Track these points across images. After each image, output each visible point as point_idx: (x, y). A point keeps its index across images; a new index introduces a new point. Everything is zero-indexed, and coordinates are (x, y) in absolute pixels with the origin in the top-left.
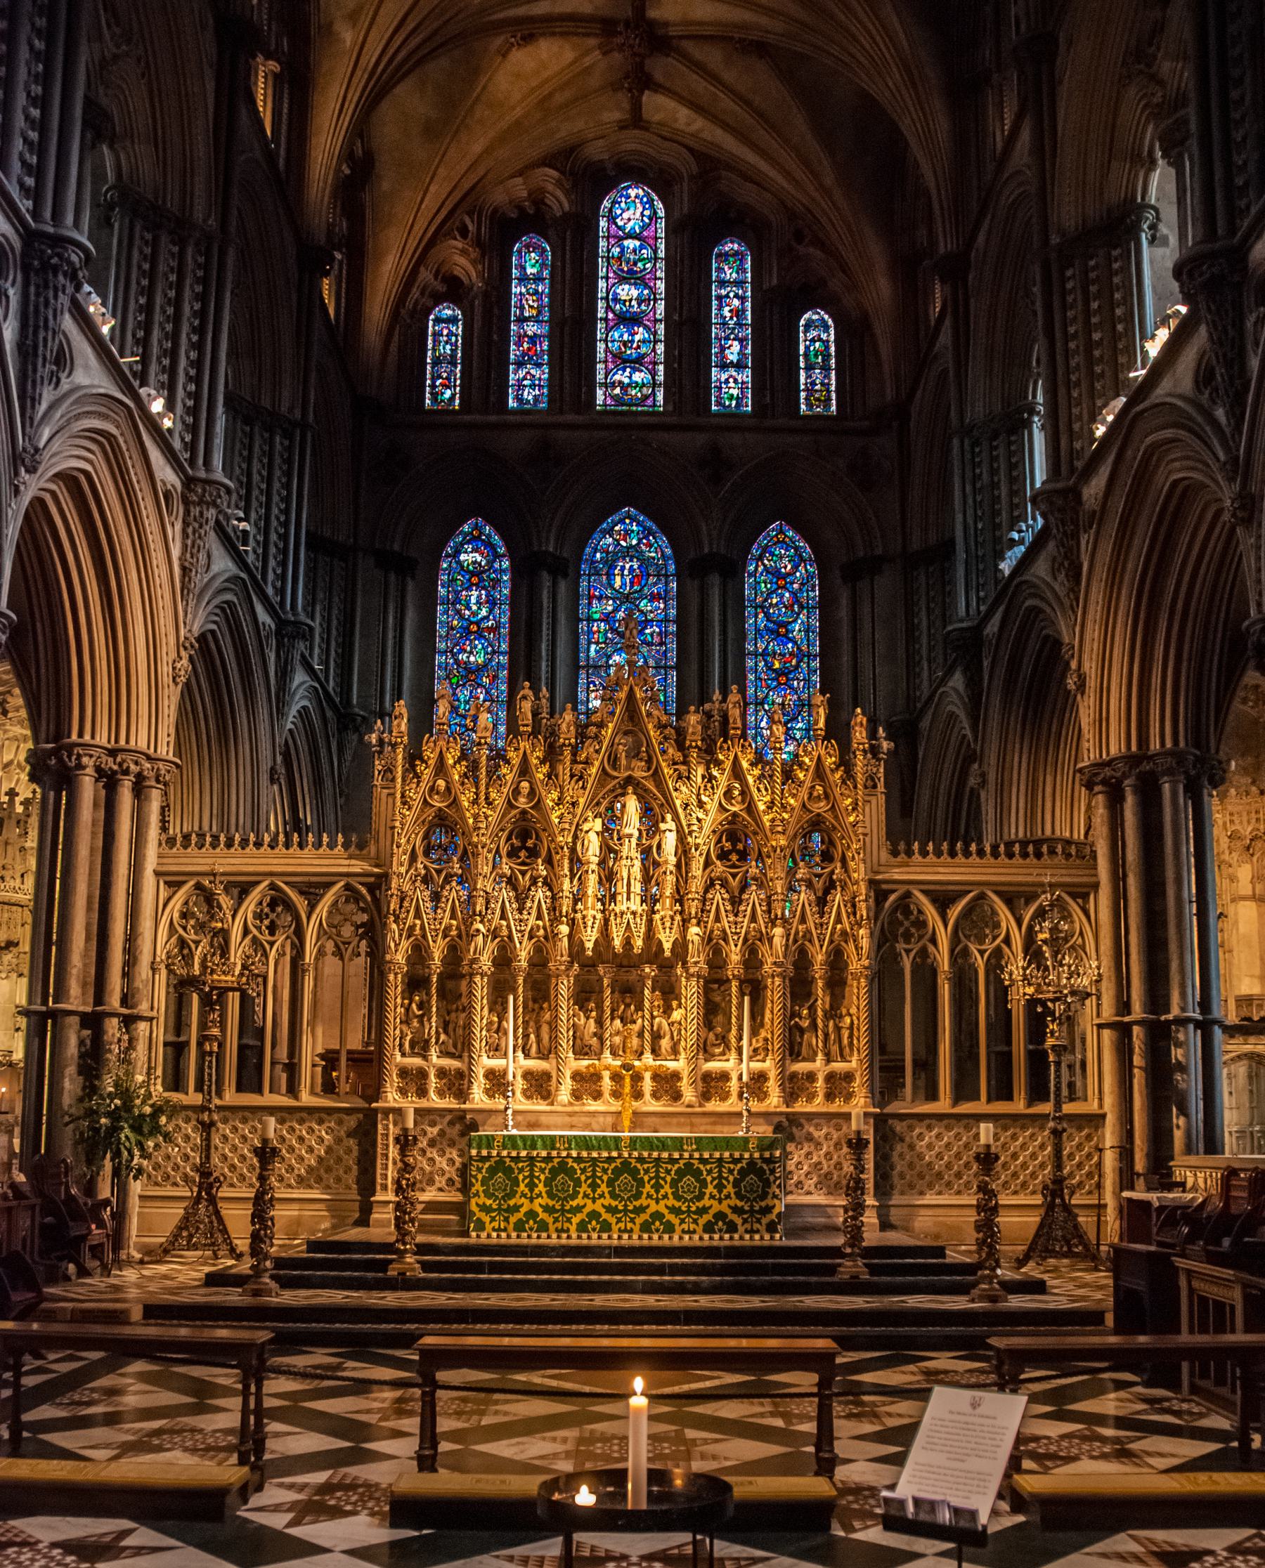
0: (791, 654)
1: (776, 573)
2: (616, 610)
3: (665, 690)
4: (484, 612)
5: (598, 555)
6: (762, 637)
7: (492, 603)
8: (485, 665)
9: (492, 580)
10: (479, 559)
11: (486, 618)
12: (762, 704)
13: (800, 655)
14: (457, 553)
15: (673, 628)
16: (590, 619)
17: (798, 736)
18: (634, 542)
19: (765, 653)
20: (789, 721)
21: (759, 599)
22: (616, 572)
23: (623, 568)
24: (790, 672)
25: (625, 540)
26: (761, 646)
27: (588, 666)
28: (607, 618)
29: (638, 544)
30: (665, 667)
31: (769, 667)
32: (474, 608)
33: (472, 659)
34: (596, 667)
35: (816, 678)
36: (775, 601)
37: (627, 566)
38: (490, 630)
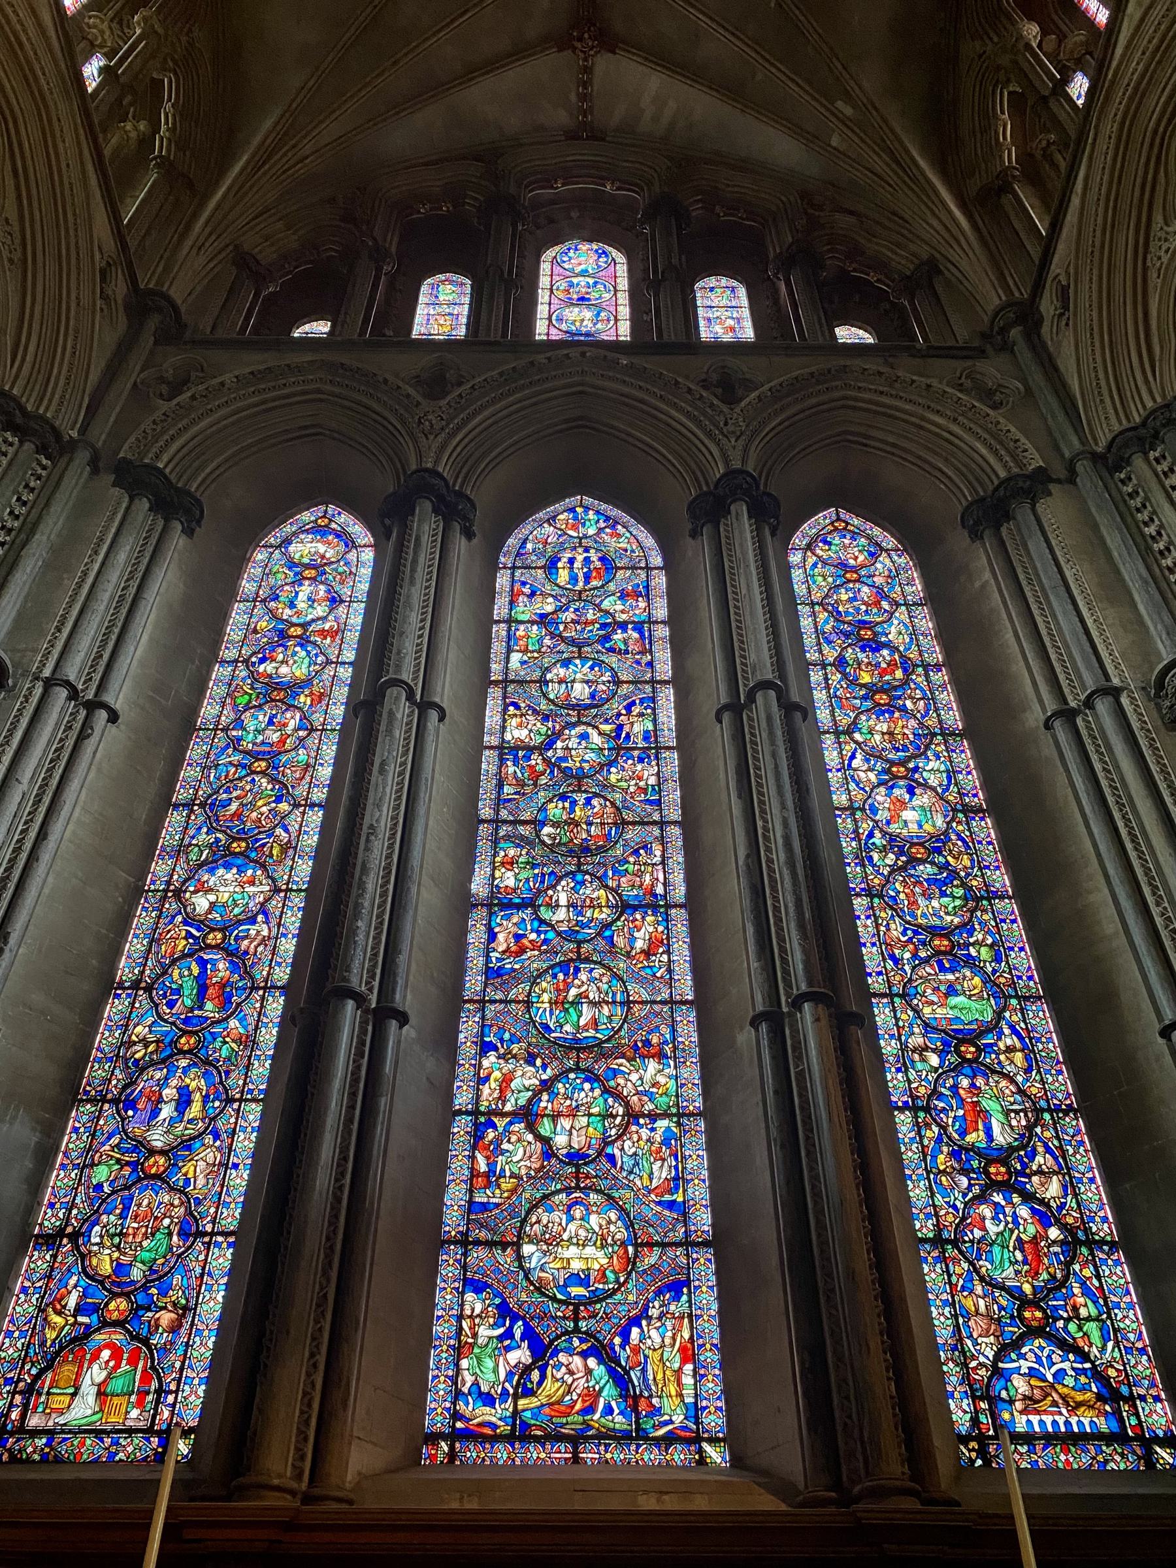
0: (892, 664)
1: (843, 565)
2: (559, 610)
3: (654, 714)
4: (320, 610)
5: (529, 546)
6: (830, 642)
7: (334, 601)
8: (308, 682)
9: (340, 574)
10: (322, 551)
11: (324, 619)
12: (849, 732)
13: (908, 667)
14: (287, 542)
15: (662, 632)
16: (510, 621)
17: (933, 781)
18: (592, 531)
19: (840, 662)
20: (909, 759)
21: (817, 596)
22: (560, 565)
23: (571, 561)
24: (895, 688)
25: (577, 529)
26: (831, 655)
27: (506, 682)
28: (543, 620)
29: (598, 534)
30: (653, 682)
31: (854, 682)
32: (301, 605)
33: (284, 670)
34: (521, 682)
35: (947, 697)
36: (844, 597)
37: (580, 558)
38: (323, 633)
